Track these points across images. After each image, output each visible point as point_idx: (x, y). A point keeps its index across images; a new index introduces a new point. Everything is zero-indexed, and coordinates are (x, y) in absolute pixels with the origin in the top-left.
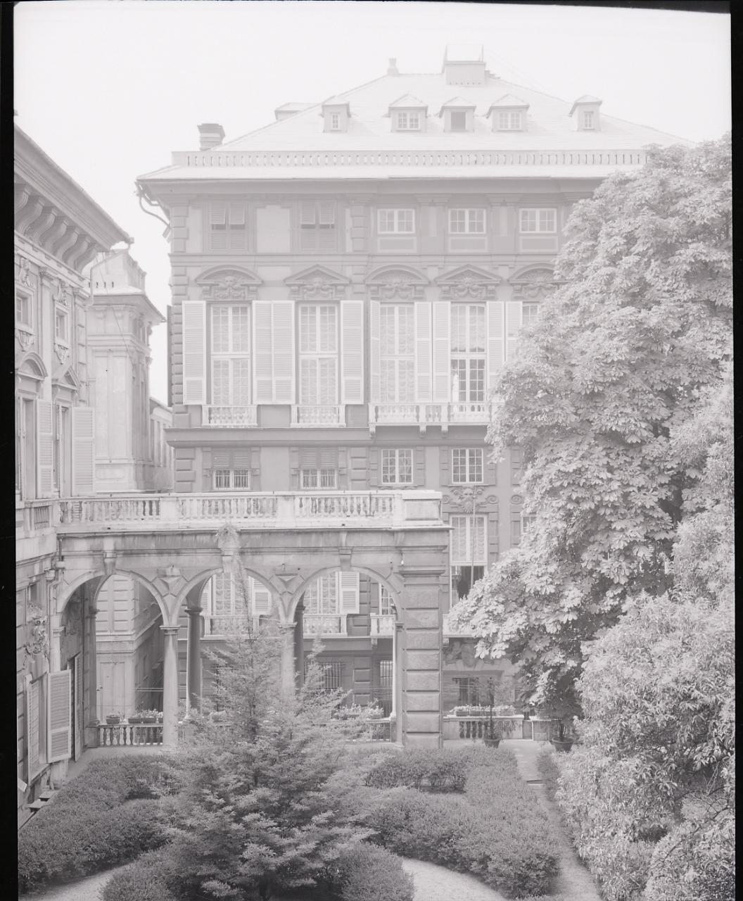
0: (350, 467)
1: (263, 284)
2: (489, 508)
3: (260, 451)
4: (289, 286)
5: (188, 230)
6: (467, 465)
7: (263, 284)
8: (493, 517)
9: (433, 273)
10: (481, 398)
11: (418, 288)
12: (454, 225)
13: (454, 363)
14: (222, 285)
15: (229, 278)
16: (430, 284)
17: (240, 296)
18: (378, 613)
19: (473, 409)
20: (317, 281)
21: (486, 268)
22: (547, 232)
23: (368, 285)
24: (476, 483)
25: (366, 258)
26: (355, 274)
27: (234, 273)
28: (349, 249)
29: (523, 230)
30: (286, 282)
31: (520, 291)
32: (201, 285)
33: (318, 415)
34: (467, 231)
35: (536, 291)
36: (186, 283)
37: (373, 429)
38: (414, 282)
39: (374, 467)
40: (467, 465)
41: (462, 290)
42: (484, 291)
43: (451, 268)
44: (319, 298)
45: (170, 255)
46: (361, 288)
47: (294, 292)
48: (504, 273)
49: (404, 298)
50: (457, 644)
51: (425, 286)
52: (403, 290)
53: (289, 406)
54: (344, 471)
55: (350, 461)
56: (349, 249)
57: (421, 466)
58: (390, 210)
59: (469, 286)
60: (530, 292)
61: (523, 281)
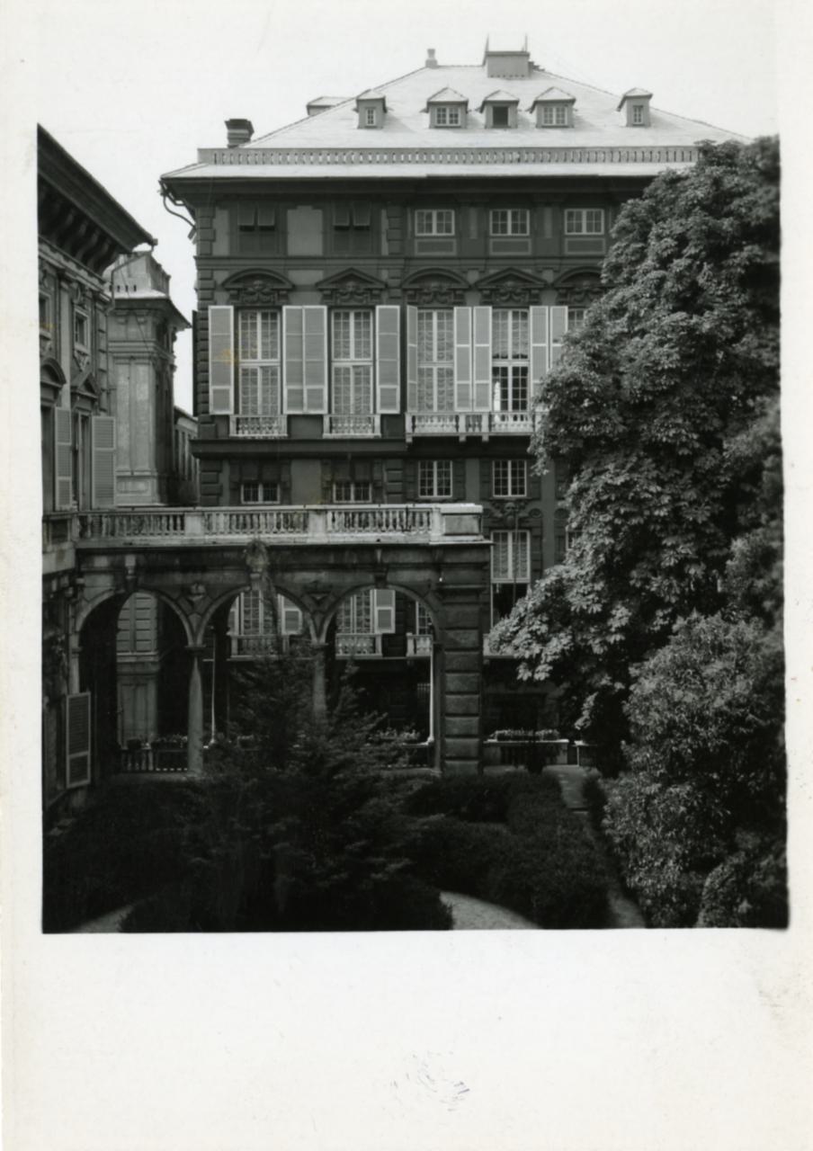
0: (385, 479)
1: (294, 288)
2: (532, 522)
3: (289, 465)
4: (321, 290)
5: (215, 233)
6: (510, 478)
7: (294, 288)
8: (537, 532)
9: (473, 277)
10: (524, 407)
12: (495, 226)
13: (495, 370)
14: (251, 289)
15: (258, 282)
16: (470, 288)
17: (269, 302)
18: (414, 633)
19: (515, 418)
20: (350, 285)
21: (529, 271)
22: (594, 233)
24: (518, 496)
25: (402, 262)
26: (393, 278)
27: (263, 277)
29: (569, 231)
30: (317, 287)
31: (565, 295)
32: (228, 290)
33: (352, 425)
34: (509, 233)
35: (582, 295)
36: (212, 286)
37: (409, 440)
38: (454, 286)
39: (411, 479)
40: (510, 478)
42: (527, 296)
43: (492, 271)
44: (353, 303)
45: (196, 258)
46: (398, 292)
47: (325, 297)
48: (549, 276)
49: (443, 303)
51: (465, 290)
52: (443, 294)
53: (320, 417)
54: (380, 484)
55: (385, 474)
56: (385, 251)
58: (429, 211)
59: (511, 290)
60: (577, 297)
61: (570, 285)
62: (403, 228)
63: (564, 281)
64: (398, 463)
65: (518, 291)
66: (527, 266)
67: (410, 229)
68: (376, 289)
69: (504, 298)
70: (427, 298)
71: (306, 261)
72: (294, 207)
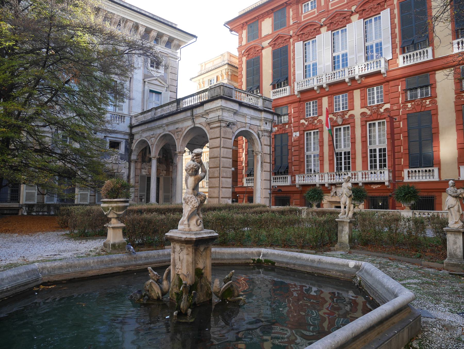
2: (351, 121)
7: (263, 48)
9: (323, 20)
11: (317, 29)
16: (322, 26)
20: (279, 41)
21: (346, 10)
23: (298, 36)
28: (291, 23)
30: (270, 45)
32: (245, 56)
37: (296, 93)
39: (302, 110)
46: (296, 37)
50: (333, 187)
56: (291, 23)
57: (320, 107)
61: (362, 8)
64: (296, 105)
65: (341, 20)
66: (345, 8)
70: (307, 36)
71: (267, 37)
72: (264, 20)
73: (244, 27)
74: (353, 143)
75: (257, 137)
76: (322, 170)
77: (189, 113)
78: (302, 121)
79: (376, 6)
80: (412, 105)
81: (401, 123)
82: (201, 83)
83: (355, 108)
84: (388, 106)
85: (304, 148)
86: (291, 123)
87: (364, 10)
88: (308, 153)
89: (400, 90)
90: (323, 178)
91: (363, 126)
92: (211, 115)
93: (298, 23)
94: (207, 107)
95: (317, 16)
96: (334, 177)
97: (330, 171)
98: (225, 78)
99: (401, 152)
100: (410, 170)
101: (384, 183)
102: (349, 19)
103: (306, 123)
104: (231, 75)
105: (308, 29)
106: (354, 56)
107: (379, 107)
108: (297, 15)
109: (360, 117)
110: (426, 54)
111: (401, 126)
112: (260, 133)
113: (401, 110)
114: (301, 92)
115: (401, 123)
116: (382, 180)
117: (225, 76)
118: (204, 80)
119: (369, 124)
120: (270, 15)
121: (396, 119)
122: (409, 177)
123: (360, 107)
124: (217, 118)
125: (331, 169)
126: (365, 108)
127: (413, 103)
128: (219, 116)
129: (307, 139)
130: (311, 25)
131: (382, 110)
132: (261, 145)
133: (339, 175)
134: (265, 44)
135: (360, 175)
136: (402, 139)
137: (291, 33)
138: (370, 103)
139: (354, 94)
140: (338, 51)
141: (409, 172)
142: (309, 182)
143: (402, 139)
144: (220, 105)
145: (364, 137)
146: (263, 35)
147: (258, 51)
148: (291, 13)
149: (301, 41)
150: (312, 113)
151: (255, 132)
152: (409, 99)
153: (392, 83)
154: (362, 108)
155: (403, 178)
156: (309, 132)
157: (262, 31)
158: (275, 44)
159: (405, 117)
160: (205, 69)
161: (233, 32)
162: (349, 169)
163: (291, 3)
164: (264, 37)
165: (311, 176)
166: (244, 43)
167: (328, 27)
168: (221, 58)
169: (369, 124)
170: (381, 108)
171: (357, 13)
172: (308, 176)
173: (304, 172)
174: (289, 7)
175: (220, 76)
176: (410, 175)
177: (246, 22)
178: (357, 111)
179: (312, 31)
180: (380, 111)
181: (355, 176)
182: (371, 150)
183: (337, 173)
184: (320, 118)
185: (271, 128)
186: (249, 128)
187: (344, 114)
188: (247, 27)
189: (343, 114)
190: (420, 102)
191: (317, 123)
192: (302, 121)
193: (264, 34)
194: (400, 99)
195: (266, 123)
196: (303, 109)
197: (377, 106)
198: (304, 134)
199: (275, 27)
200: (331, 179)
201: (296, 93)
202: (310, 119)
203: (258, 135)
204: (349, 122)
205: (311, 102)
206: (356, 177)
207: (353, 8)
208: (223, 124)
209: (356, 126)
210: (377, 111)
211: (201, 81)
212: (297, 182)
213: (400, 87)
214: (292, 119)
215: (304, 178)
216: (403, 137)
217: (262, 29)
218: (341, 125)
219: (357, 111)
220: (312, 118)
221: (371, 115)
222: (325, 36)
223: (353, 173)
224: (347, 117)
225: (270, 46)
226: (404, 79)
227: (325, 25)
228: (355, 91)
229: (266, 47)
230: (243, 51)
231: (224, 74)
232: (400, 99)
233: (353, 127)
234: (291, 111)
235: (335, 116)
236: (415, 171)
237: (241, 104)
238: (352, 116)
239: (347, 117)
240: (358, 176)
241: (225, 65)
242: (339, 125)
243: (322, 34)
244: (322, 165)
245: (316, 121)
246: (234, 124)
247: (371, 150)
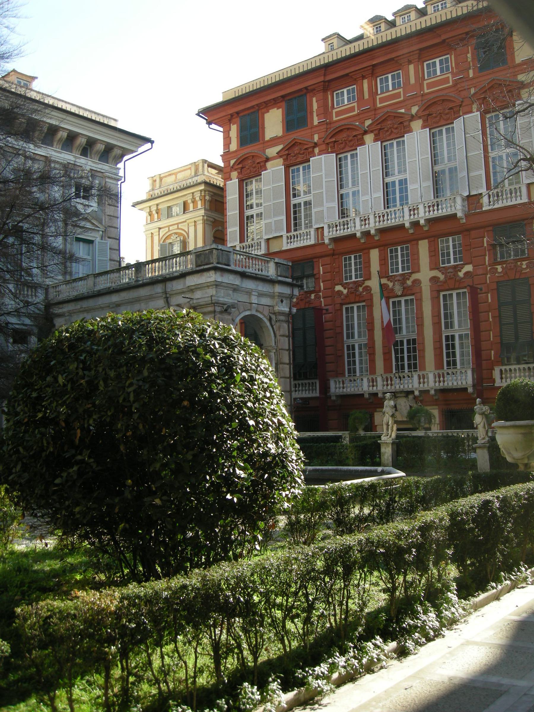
0: (321, 273)
7: (268, 159)
9: (368, 123)
16: (365, 132)
20: (296, 149)
21: (403, 111)
23: (328, 144)
28: (316, 122)
30: (279, 154)
32: (236, 170)
37: (327, 241)
38: (355, 133)
39: (337, 270)
41: (387, 131)
46: (323, 147)
52: (351, 141)
55: (321, 268)
56: (316, 122)
59: (390, 127)
61: (427, 112)
62: (326, 106)
63: (424, 110)
64: (327, 260)
65: (396, 126)
67: (330, 105)
68: (310, 147)
69: (388, 133)
70: (342, 146)
71: (274, 141)
72: (268, 112)
73: (234, 120)
74: (421, 325)
75: (268, 324)
76: (373, 371)
77: (159, 288)
78: (338, 288)
79: (447, 111)
80: (502, 268)
81: (489, 295)
82: (154, 212)
83: (421, 269)
84: (469, 268)
85: (342, 333)
86: (320, 291)
87: (429, 115)
88: (351, 341)
89: (485, 245)
90: (375, 383)
91: (435, 299)
92: (198, 295)
93: (327, 124)
94: (191, 281)
95: (358, 114)
96: (391, 380)
97: (385, 372)
98: (199, 206)
99: (490, 340)
100: (503, 368)
101: (466, 389)
102: (409, 126)
103: (345, 292)
104: (210, 202)
105: (344, 135)
106: (417, 186)
107: (457, 268)
108: (325, 110)
109: (429, 284)
110: (518, 194)
111: (490, 301)
112: (273, 317)
113: (488, 276)
114: (335, 240)
115: (489, 295)
116: (464, 385)
117: (199, 203)
118: (160, 207)
119: (444, 295)
120: (278, 105)
121: (481, 289)
122: (502, 378)
123: (428, 268)
124: (210, 299)
125: (388, 369)
126: (437, 271)
127: (504, 266)
128: (211, 296)
129: (347, 317)
130: (348, 129)
131: (461, 274)
132: (275, 336)
133: (400, 377)
134: (272, 152)
135: (431, 376)
136: (491, 320)
137: (316, 138)
138: (443, 263)
139: (420, 247)
140: (393, 175)
141: (501, 371)
142: (353, 389)
143: (491, 320)
144: (212, 279)
145: (436, 315)
146: (267, 138)
147: (258, 163)
148: (315, 106)
149: (332, 152)
150: (353, 274)
151: (265, 316)
152: (499, 260)
153: (473, 233)
154: (431, 269)
155: (494, 381)
156: (349, 306)
157: (266, 130)
158: (288, 154)
159: (494, 286)
160: (160, 187)
161: (213, 126)
162: (415, 367)
163: (314, 89)
164: (268, 141)
165: (355, 381)
166: (234, 146)
167: (376, 135)
168: (190, 169)
169: (444, 295)
170: (460, 271)
171: (420, 118)
172: (351, 381)
173: (343, 374)
174: (311, 94)
175: (189, 201)
176: (503, 376)
177: (238, 113)
178: (425, 274)
179: (350, 138)
180: (458, 276)
181: (424, 378)
182: (447, 337)
183: (397, 375)
184: (367, 283)
185: (290, 309)
186: (257, 311)
187: (404, 278)
188: (238, 120)
189: (403, 279)
190: (513, 265)
191: (363, 292)
192: (338, 288)
193: (269, 135)
194: (487, 258)
195: (282, 301)
196: (340, 267)
197: (455, 267)
198: (341, 310)
199: (290, 124)
200: (387, 385)
201: (327, 241)
202: (351, 286)
203: (270, 320)
204: (412, 291)
205: (353, 257)
206: (426, 380)
207: (414, 110)
208: (218, 309)
209: (424, 299)
210: (454, 275)
211: (154, 209)
212: (333, 389)
213: (485, 239)
214: (322, 284)
215: (343, 383)
216: (492, 317)
217: (266, 126)
218: (402, 296)
219: (425, 274)
220: (355, 282)
221: (445, 282)
222: (370, 150)
223: (421, 373)
224: (409, 283)
225: (281, 157)
226: (490, 228)
227: (372, 132)
228: (420, 242)
229: (274, 158)
230: (232, 162)
231: (198, 199)
232: (487, 258)
233: (420, 300)
234: (319, 271)
235: (391, 282)
236: (510, 370)
237: (243, 275)
238: (417, 282)
239: (409, 283)
240: (428, 378)
241: (200, 184)
242: (397, 296)
243: (367, 146)
244: (372, 361)
245: (361, 289)
246: (233, 306)
247: (447, 337)
